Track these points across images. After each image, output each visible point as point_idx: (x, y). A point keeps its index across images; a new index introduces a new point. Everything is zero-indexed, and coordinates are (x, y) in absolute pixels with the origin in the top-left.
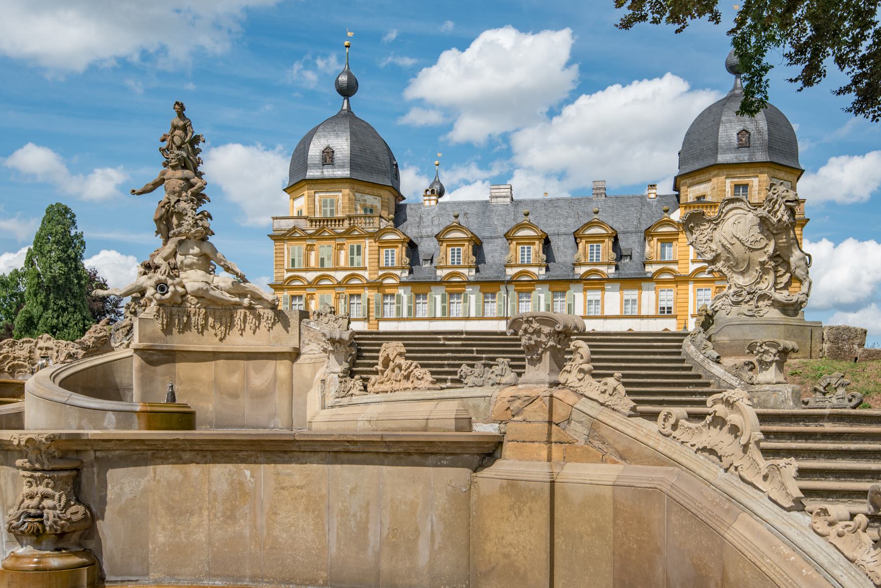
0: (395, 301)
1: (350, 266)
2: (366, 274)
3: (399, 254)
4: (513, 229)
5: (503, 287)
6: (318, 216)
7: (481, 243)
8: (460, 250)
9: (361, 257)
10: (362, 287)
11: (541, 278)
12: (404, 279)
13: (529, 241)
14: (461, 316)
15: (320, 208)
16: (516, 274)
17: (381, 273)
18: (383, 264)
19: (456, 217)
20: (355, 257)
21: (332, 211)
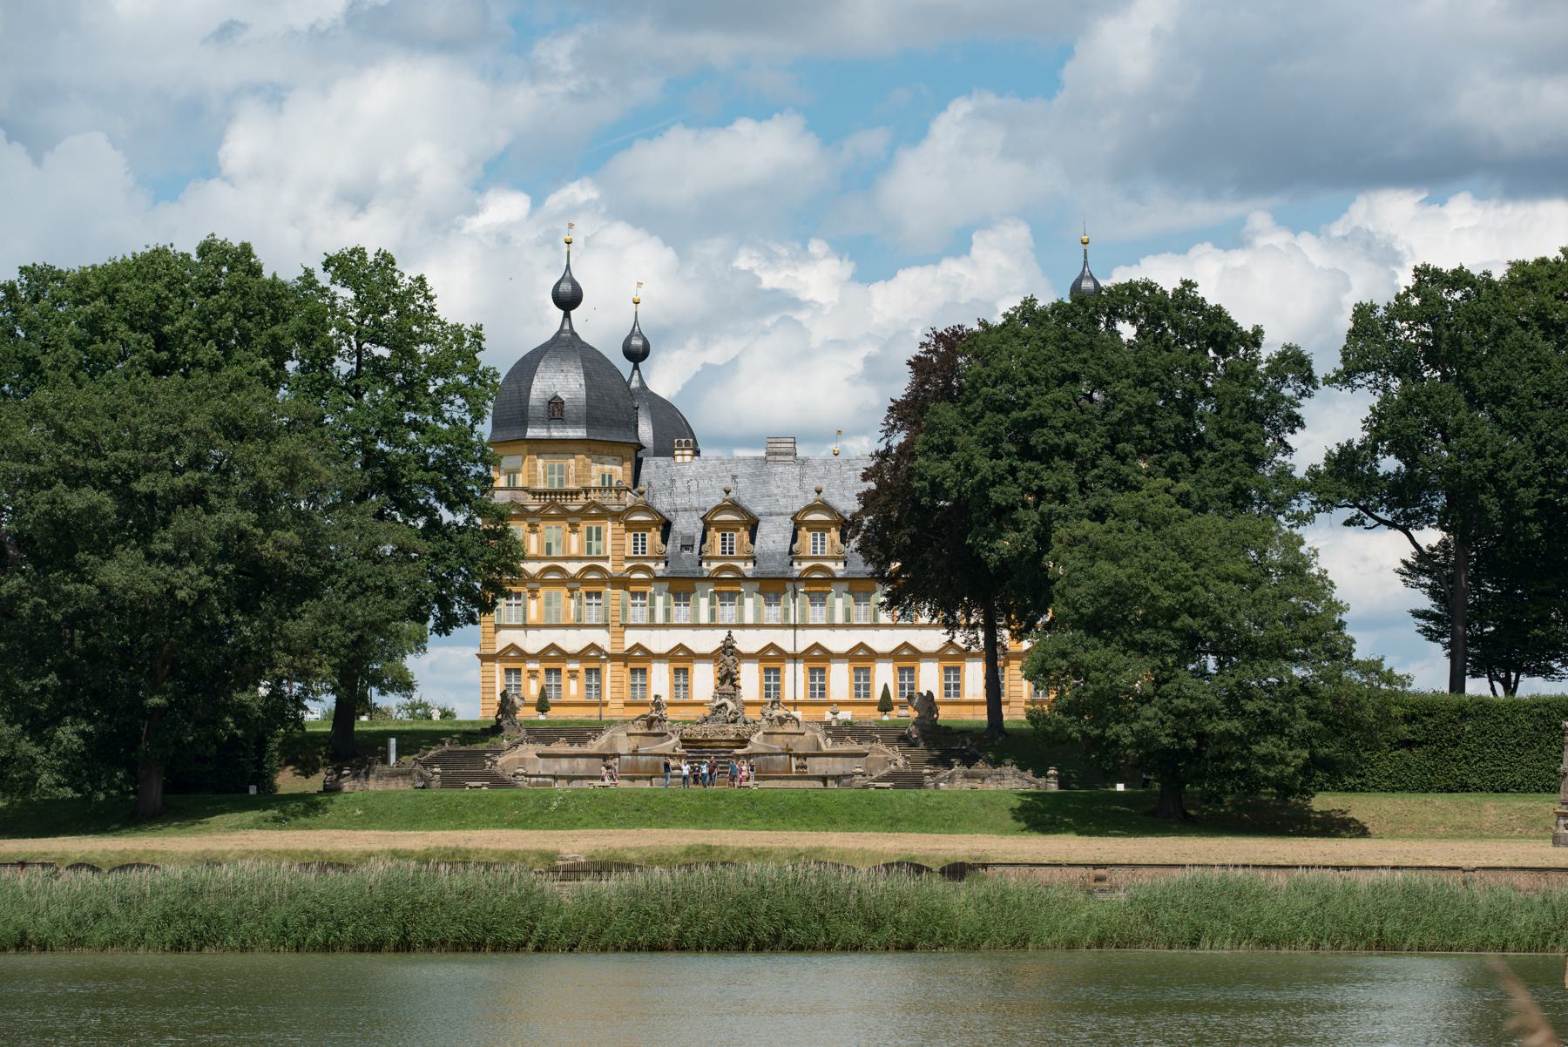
0: (647, 601)
1: (585, 555)
2: (608, 566)
3: (654, 537)
4: (802, 511)
5: (789, 586)
6: (541, 486)
7: (758, 522)
8: (731, 535)
9: (602, 543)
10: (603, 582)
11: (838, 575)
12: (659, 574)
13: (822, 527)
14: (734, 622)
15: (545, 476)
16: (807, 570)
17: (627, 565)
18: (629, 552)
19: (728, 492)
20: (594, 543)
21: (561, 481)
